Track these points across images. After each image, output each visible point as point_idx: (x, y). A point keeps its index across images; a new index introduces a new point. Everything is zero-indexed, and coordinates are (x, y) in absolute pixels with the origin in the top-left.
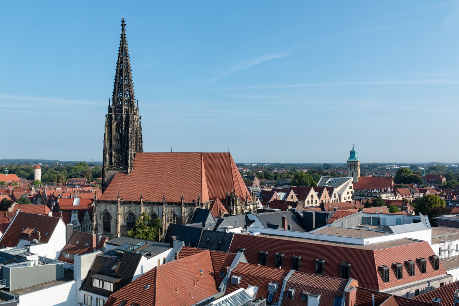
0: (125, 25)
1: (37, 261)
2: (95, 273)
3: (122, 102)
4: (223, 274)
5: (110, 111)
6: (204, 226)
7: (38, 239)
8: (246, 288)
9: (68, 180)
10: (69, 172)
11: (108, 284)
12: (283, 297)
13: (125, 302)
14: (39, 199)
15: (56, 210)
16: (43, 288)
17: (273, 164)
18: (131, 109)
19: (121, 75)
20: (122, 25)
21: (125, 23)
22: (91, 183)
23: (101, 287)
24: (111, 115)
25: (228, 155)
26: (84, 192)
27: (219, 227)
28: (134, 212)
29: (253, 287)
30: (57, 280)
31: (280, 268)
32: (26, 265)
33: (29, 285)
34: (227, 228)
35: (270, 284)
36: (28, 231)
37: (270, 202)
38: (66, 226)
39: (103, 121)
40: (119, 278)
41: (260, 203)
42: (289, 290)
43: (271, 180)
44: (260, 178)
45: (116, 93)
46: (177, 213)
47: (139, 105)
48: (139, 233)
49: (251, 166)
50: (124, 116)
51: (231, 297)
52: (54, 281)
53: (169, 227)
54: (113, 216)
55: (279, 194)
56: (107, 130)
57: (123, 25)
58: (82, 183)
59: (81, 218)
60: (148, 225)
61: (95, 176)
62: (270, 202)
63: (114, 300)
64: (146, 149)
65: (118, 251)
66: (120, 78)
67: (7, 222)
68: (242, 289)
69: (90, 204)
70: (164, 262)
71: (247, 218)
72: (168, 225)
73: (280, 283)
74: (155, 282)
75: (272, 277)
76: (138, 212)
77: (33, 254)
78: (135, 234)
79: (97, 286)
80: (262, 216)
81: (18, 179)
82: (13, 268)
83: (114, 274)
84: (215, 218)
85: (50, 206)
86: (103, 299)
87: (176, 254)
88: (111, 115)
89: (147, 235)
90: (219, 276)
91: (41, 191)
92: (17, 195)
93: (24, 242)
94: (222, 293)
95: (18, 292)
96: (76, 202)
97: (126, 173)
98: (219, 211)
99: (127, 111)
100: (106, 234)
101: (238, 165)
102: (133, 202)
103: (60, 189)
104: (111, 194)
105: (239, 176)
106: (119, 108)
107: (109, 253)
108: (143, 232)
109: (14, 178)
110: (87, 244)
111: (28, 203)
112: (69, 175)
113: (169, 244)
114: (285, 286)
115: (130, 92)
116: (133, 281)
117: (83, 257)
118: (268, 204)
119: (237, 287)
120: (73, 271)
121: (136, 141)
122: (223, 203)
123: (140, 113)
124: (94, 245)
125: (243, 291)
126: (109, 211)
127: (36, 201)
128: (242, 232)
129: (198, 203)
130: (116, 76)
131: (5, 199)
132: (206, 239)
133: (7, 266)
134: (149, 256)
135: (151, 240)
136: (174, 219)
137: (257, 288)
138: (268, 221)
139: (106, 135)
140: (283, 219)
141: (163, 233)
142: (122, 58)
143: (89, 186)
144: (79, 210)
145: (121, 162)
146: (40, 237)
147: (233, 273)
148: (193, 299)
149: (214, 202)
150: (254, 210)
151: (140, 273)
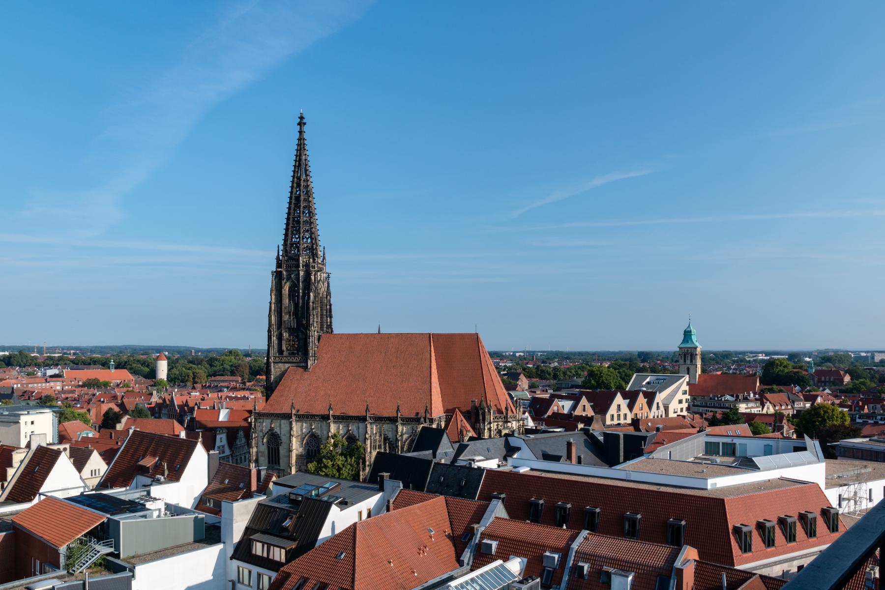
1: (163, 510)
4: (467, 535)
6: (434, 456)
7: (163, 475)
8: (506, 559)
9: (210, 379)
10: (211, 366)
12: (570, 576)
14: (164, 411)
15: (191, 428)
22: (248, 384)
26: (236, 398)
28: (319, 432)
29: (519, 560)
32: (145, 516)
33: (149, 550)
35: (548, 554)
36: (149, 462)
38: (209, 455)
42: (580, 564)
48: (326, 467)
51: (482, 575)
53: (376, 457)
54: (284, 439)
56: (273, 297)
58: (233, 384)
60: (341, 454)
61: (255, 372)
65: (293, 497)
67: (116, 447)
69: (246, 420)
70: (369, 516)
72: (374, 454)
73: (565, 552)
75: (551, 542)
76: (325, 432)
77: (155, 499)
81: (131, 377)
82: (125, 521)
85: (181, 422)
87: (389, 501)
89: (339, 470)
90: (460, 540)
91: (168, 397)
93: (141, 479)
94: (466, 568)
95: (133, 561)
96: (223, 415)
97: (306, 368)
100: (273, 469)
102: (317, 416)
103: (198, 394)
107: (278, 499)
108: (333, 465)
109: (125, 375)
110: (241, 485)
111: (146, 416)
112: (211, 370)
113: (377, 486)
114: (573, 558)
119: (491, 559)
121: (322, 315)
124: (254, 487)
125: (502, 565)
126: (277, 430)
127: (160, 413)
131: (110, 409)
132: (439, 478)
133: (116, 518)
134: (344, 504)
135: (346, 479)
136: (385, 444)
137: (525, 560)
139: (273, 306)
141: (367, 469)
143: (243, 389)
144: (228, 428)
145: (298, 349)
146: (166, 472)
147: (484, 535)
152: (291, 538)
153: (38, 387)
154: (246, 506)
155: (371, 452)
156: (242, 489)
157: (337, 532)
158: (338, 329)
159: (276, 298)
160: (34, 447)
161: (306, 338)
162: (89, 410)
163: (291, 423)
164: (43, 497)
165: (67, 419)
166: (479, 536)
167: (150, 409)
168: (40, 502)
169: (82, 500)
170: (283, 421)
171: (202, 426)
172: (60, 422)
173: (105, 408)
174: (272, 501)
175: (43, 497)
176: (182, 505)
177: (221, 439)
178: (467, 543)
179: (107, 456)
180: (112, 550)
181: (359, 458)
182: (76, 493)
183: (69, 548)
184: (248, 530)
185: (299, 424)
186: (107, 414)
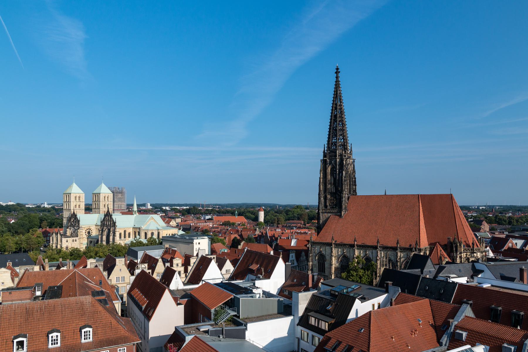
0: (339, 72)
1: (261, 294)
2: (311, 311)
3: (336, 147)
4: (445, 326)
5: (325, 156)
7: (262, 275)
8: (473, 345)
10: (287, 214)
11: (323, 323)
13: (340, 343)
16: (266, 319)
17: (507, 206)
18: (345, 153)
19: (335, 121)
20: (336, 73)
21: (339, 70)
22: (307, 225)
23: (316, 325)
24: (326, 160)
25: (450, 197)
27: (440, 275)
28: (348, 255)
29: (483, 347)
30: (279, 313)
31: (519, 328)
32: (252, 297)
33: (254, 315)
34: (449, 277)
35: (505, 345)
36: (254, 267)
37: (503, 250)
38: (285, 265)
39: (318, 166)
40: (333, 317)
41: (490, 251)
43: (504, 225)
44: (489, 222)
45: (331, 138)
46: (393, 258)
47: (353, 149)
48: (353, 276)
49: (478, 208)
50: (338, 160)
52: (275, 314)
54: (327, 258)
55: (515, 241)
56: (322, 174)
57: (337, 72)
58: (299, 225)
59: (298, 259)
60: (362, 269)
61: (311, 218)
62: (503, 250)
63: (329, 339)
64: (361, 191)
66: (334, 123)
67: (238, 258)
68: (468, 346)
69: (306, 246)
70: (379, 307)
71: (473, 267)
72: (382, 269)
74: (370, 326)
75: (508, 337)
76: (352, 255)
77: (258, 288)
78: (349, 276)
79: (313, 323)
80: (493, 265)
82: (243, 298)
83: (328, 314)
84: (434, 265)
85: (271, 246)
86: (318, 338)
87: (392, 300)
88: (326, 160)
90: (440, 329)
91: (264, 232)
92: (245, 234)
95: (246, 320)
96: (293, 243)
97: (340, 216)
98: (440, 257)
99: (341, 155)
100: (321, 275)
101: (463, 208)
102: (347, 245)
103: (280, 230)
104: (326, 236)
105: (464, 220)
106: (333, 152)
107: (324, 293)
108: (357, 275)
110: (303, 283)
111: (253, 242)
113: (384, 290)
115: (344, 136)
116: (347, 322)
117: (300, 294)
118: (501, 252)
119: (463, 344)
120: (291, 307)
122: (444, 250)
123: (353, 157)
124: (310, 285)
125: (469, 349)
126: (323, 252)
127: (260, 240)
128: (468, 282)
129: (416, 248)
130: (331, 122)
131: (235, 237)
132: (425, 287)
133: (238, 296)
135: (365, 284)
136: (389, 264)
137: (488, 347)
138: (502, 272)
140: (522, 271)
141: (378, 279)
142: (336, 104)
143: (305, 228)
144: (296, 250)
145: (336, 205)
146: (263, 274)
147: (456, 327)
148: (410, 350)
149: (434, 248)
150: (483, 259)
151: (355, 317)
152: (331, 317)
153: (201, 225)
154: (306, 295)
155: (380, 268)
156: (304, 286)
157: (359, 316)
158: (359, 192)
160: (200, 256)
161: (341, 198)
162: (225, 238)
163: (332, 249)
164: (204, 282)
165: (215, 242)
166: (453, 327)
167: (255, 238)
168: (203, 285)
169: (221, 285)
170: (327, 247)
171: (282, 248)
172: (211, 244)
173: (233, 237)
174: (321, 293)
175: (204, 282)
176: (271, 292)
177: (292, 256)
178: (445, 331)
179: (234, 263)
180: (236, 313)
181: (373, 271)
182: (219, 281)
183: (215, 311)
184: (307, 310)
185: (337, 249)
186: (234, 240)
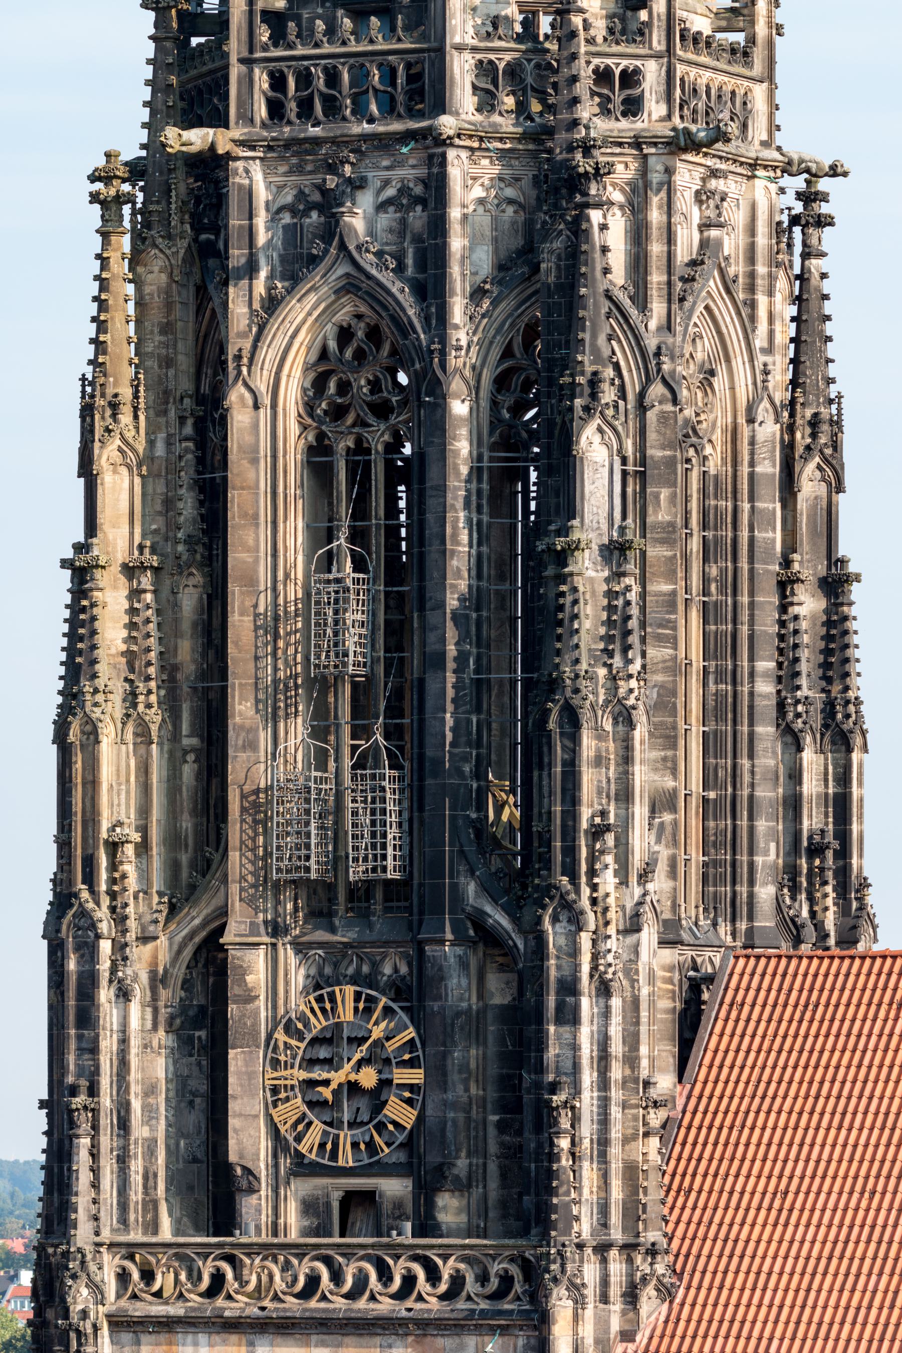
24: (210, 167)
50: (472, 184)
56: (119, 489)
88: (210, 167)
121: (727, 712)
139: (112, 599)
159: (159, 507)
